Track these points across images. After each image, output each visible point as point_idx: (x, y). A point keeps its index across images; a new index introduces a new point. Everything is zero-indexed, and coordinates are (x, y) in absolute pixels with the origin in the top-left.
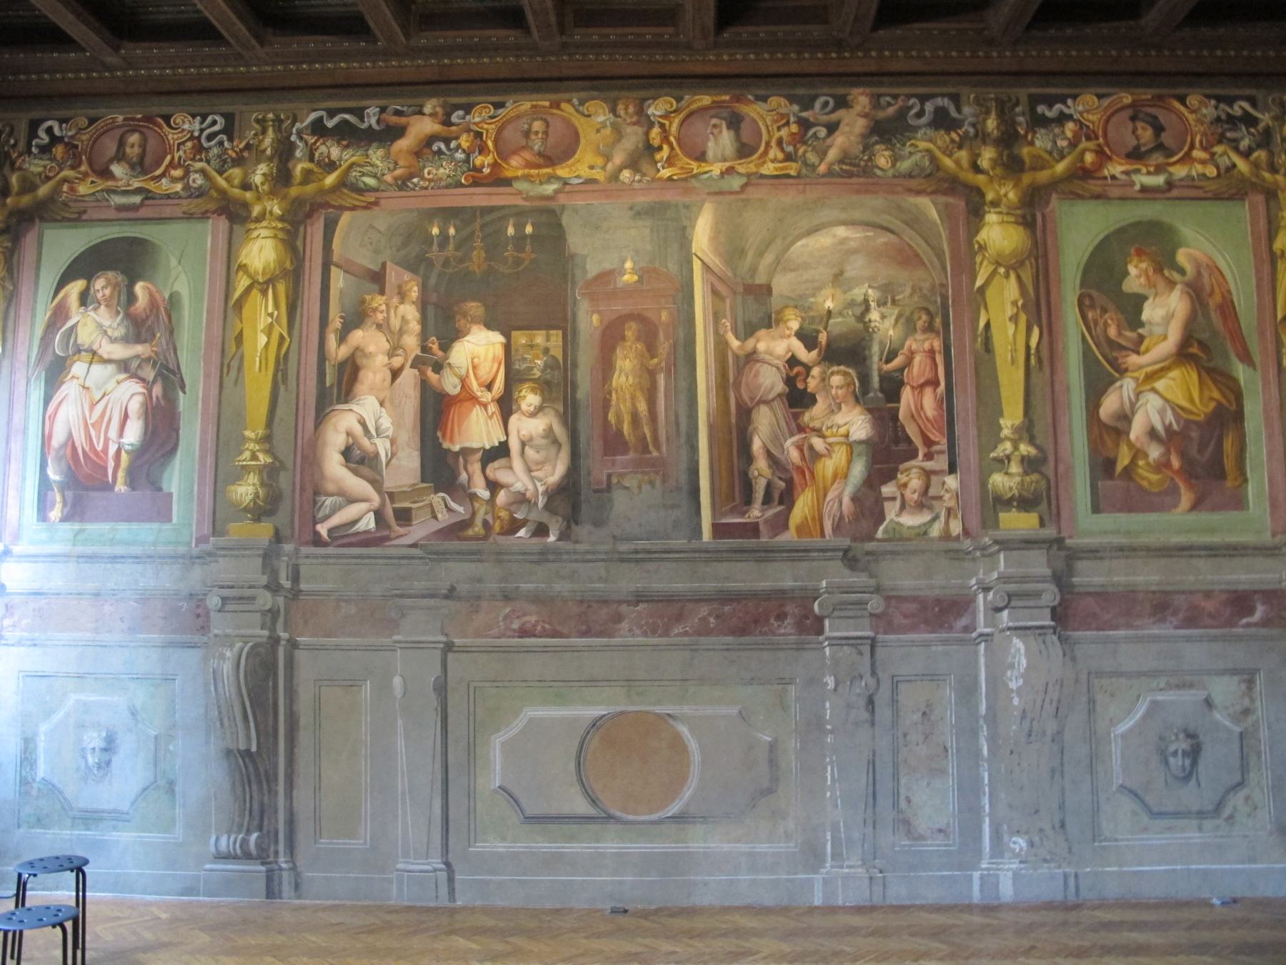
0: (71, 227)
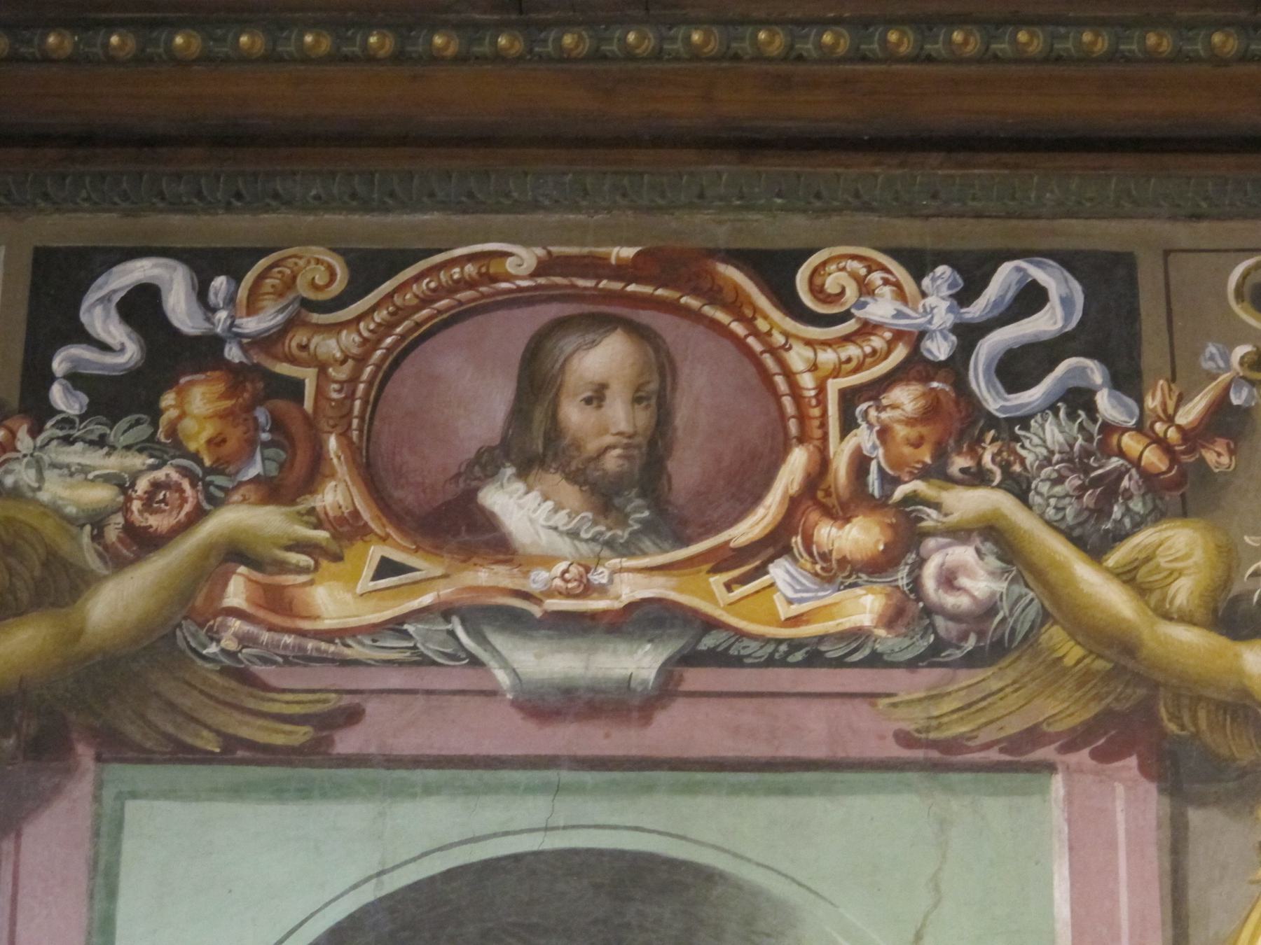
0: (279, 793)
